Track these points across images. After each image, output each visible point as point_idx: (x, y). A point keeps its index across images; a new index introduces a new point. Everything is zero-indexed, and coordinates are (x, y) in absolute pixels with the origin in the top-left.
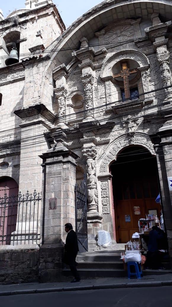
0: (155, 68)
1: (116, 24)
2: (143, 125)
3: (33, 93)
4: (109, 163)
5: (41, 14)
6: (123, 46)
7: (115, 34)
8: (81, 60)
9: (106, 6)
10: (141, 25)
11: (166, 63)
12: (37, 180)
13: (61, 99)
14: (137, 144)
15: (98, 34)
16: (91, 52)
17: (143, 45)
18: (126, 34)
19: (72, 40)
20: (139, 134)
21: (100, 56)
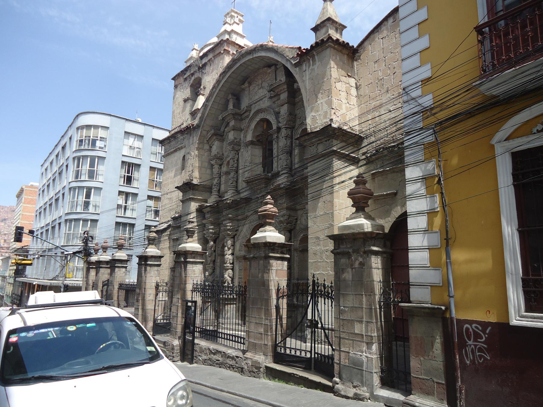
5: (217, 52)
15: (243, 87)
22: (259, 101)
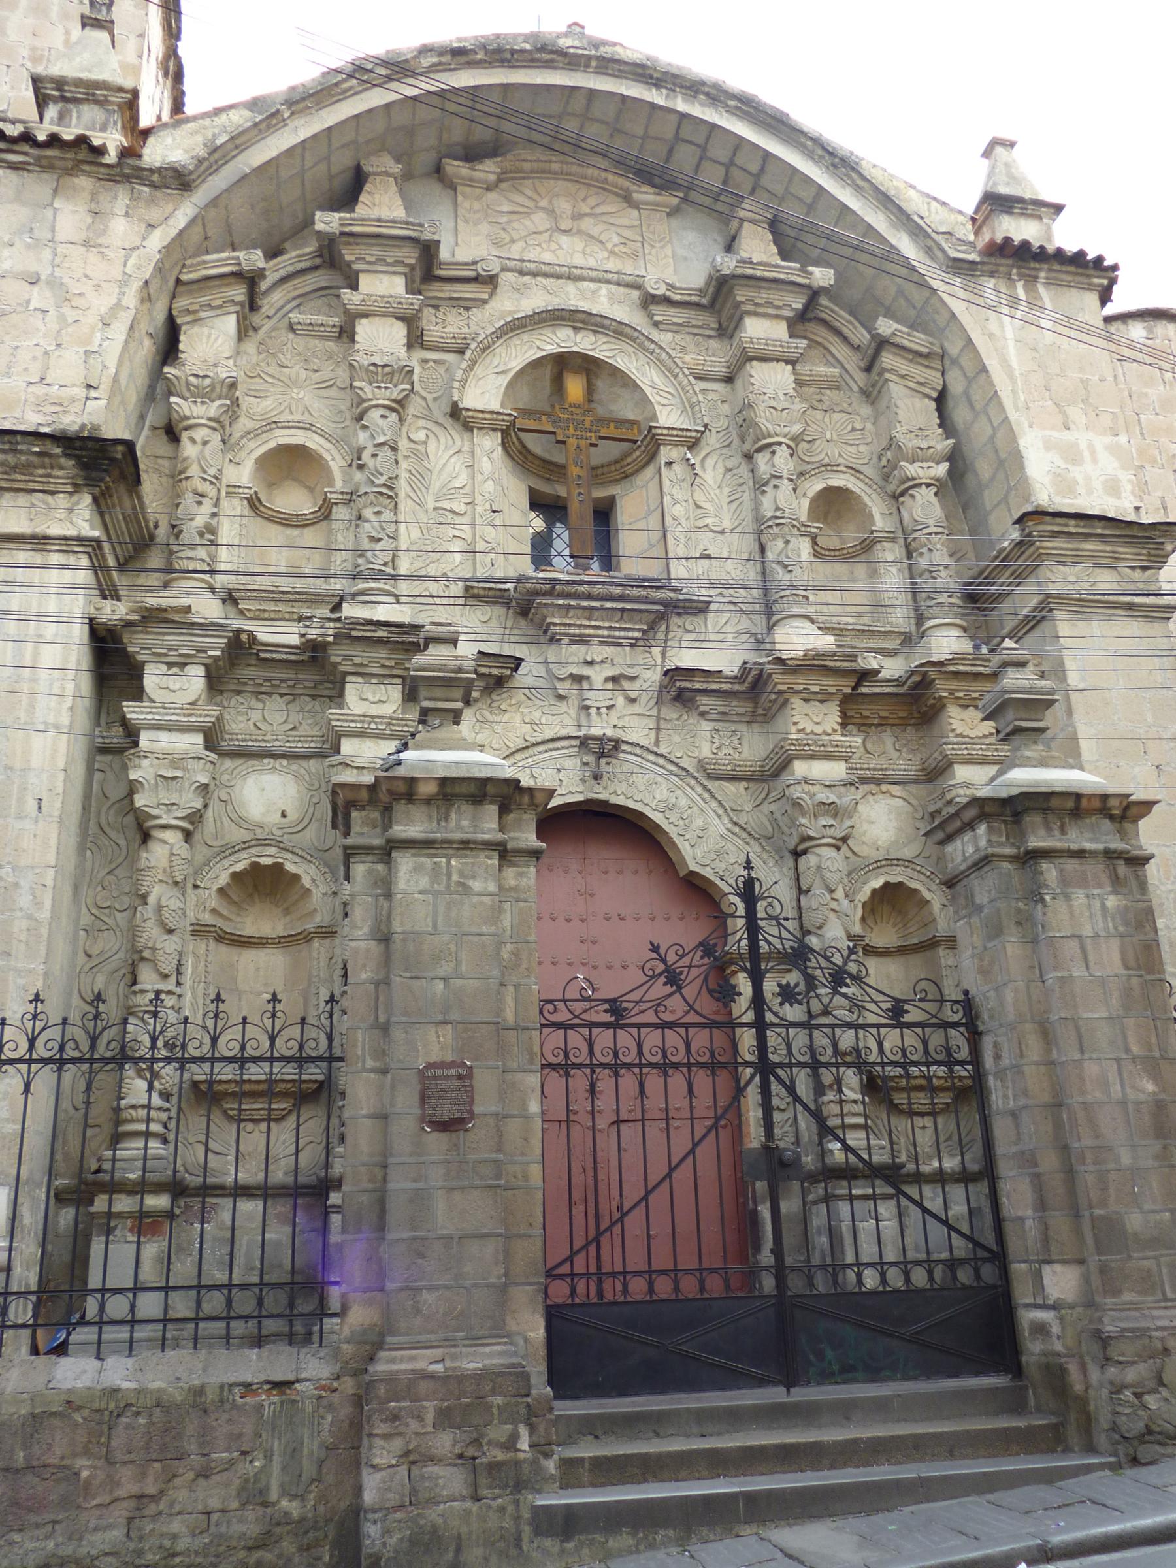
0: (724, 451)
1: (556, 167)
2: (654, 712)
3: (46, 353)
6: (580, 284)
7: (543, 209)
8: (356, 267)
9: (552, 61)
10: (675, 222)
11: (789, 447)
12: (29, 917)
13: (205, 443)
14: (621, 801)
15: (455, 168)
16: (428, 251)
17: (680, 321)
18: (602, 238)
19: (330, 145)
20: (638, 751)
21: (458, 286)
22: (558, 277)
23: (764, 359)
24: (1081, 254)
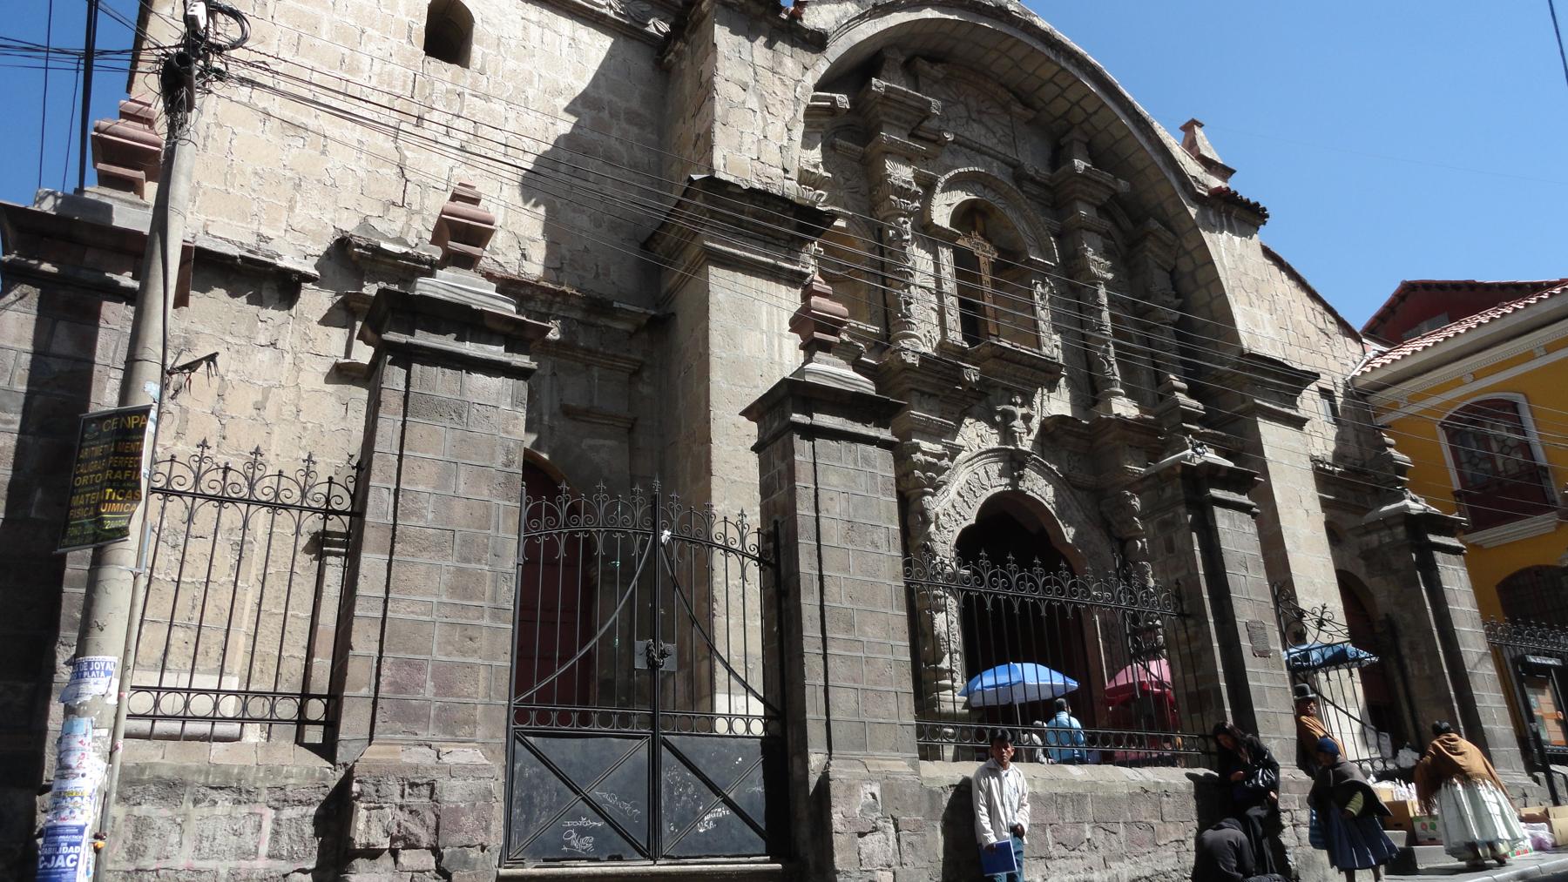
4: (958, 531)
15: (923, 66)
23: (1088, 230)
24: (1257, 204)
